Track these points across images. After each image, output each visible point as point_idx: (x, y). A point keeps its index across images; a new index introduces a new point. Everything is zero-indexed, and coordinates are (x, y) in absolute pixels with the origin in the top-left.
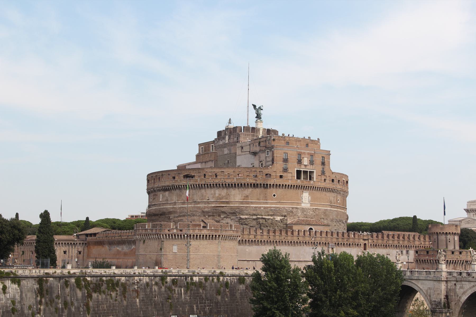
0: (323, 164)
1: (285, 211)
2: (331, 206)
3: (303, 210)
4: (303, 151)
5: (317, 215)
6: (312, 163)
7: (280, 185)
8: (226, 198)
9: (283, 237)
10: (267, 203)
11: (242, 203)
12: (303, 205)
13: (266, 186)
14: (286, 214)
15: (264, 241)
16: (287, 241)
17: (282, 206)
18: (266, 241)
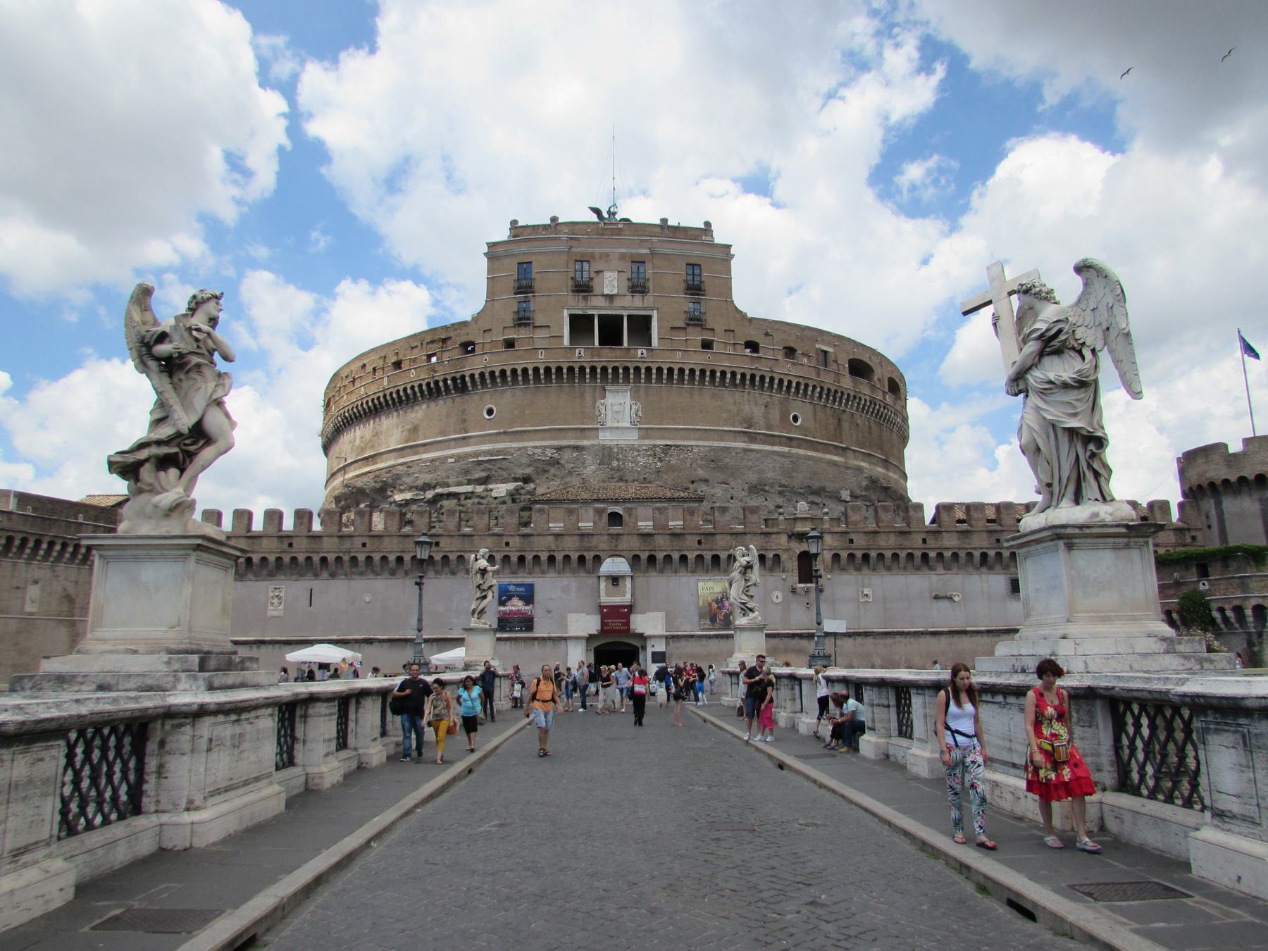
0: (695, 289)
1: (525, 460)
2: (752, 438)
3: (606, 454)
4: (597, 250)
5: (671, 468)
6: (638, 288)
7: (503, 372)
8: (373, 447)
9: (358, 542)
12: (601, 435)
13: (460, 386)
14: (528, 471)
15: (264, 559)
16: (377, 557)
17: (515, 445)
18: (272, 558)
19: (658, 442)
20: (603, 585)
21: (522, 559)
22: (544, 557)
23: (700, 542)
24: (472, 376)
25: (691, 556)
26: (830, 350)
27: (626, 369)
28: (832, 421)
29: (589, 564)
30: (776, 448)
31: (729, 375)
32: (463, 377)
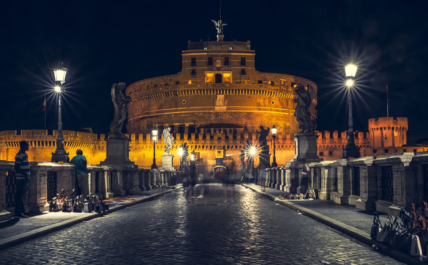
3: (217, 114)
10: (177, 110)
11: (158, 112)
12: (216, 109)
19: (232, 111)
20: (216, 153)
21: (196, 147)
22: (201, 145)
23: (240, 143)
24: (179, 92)
25: (238, 146)
26: (285, 80)
27: (223, 90)
28: (285, 102)
29: (213, 148)
30: (266, 112)
31: (253, 91)
32: (176, 92)
